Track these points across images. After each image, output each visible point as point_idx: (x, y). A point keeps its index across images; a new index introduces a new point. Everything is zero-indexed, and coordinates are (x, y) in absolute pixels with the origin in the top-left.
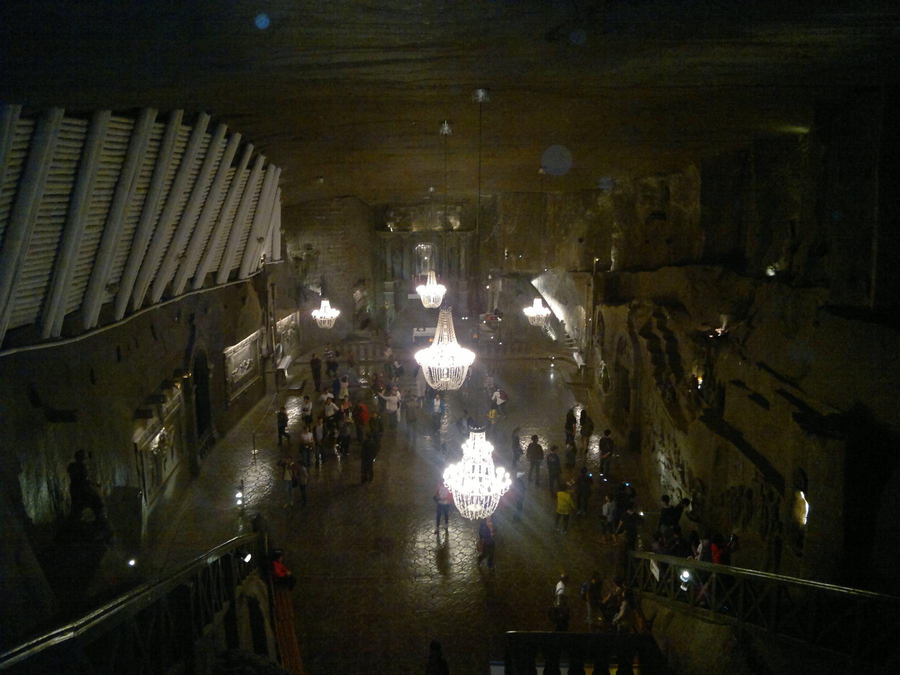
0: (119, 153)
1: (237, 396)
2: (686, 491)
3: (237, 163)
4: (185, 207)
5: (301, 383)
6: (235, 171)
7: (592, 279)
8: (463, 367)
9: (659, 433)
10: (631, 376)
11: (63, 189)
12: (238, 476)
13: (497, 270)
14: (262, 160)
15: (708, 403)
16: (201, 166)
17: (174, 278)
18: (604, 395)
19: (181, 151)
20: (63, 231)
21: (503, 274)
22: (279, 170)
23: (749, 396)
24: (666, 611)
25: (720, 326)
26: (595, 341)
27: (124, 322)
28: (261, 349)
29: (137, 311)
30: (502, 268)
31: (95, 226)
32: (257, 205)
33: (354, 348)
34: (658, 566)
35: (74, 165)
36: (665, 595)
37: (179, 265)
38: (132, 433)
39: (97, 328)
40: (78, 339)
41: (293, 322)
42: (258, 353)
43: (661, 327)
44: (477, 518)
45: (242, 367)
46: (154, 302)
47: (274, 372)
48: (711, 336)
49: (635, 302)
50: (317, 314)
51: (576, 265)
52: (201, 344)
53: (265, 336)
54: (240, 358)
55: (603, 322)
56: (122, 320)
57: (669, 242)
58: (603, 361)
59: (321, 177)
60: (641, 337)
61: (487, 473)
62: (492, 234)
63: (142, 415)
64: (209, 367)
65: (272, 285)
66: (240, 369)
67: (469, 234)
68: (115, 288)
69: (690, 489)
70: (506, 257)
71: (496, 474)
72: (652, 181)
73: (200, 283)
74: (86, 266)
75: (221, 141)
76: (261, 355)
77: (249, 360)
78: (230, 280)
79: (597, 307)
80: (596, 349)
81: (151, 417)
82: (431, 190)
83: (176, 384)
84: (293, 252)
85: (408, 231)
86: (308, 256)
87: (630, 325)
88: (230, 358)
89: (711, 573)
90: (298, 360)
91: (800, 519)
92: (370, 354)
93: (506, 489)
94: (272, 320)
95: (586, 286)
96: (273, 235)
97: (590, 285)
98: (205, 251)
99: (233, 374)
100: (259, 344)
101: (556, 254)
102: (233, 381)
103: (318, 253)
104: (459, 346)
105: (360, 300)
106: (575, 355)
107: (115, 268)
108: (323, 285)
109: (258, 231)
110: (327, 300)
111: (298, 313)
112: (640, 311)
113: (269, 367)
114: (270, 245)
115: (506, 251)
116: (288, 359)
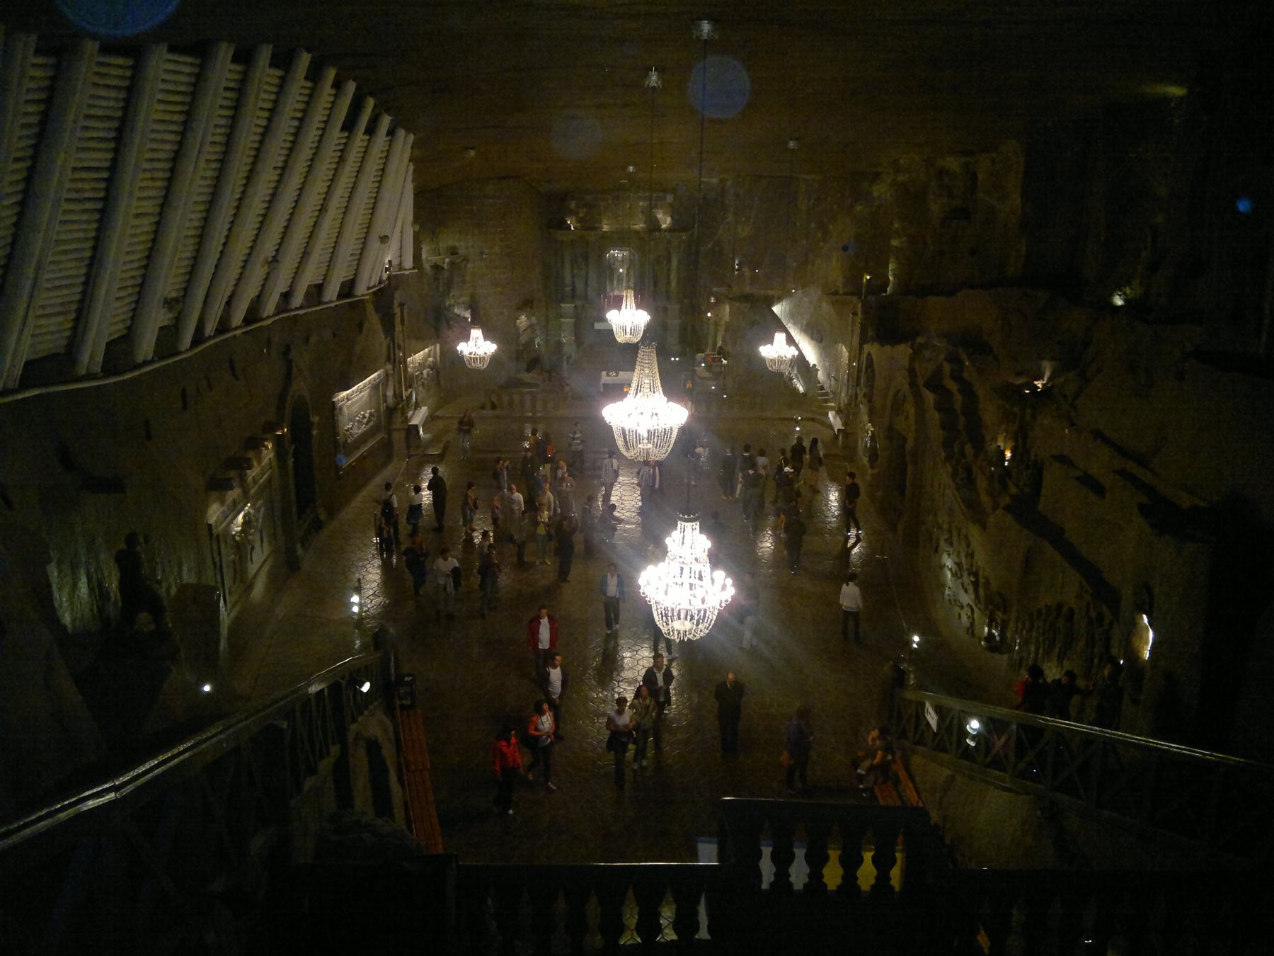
0: (178, 108)
1: (352, 463)
2: (980, 610)
3: (349, 126)
4: (276, 188)
5: (441, 445)
6: (348, 138)
7: (860, 305)
8: (671, 429)
9: (946, 526)
10: (910, 444)
11: (100, 160)
12: (354, 573)
13: (722, 290)
14: (386, 121)
15: (1017, 486)
16: (299, 129)
17: (261, 291)
18: (870, 471)
19: (269, 105)
20: (100, 221)
21: (731, 296)
22: (412, 137)
23: (1078, 479)
24: (947, 772)
25: (1040, 378)
26: (860, 397)
27: (189, 354)
28: (385, 396)
29: (210, 338)
30: (730, 286)
31: (146, 214)
32: (378, 188)
33: (516, 398)
34: (936, 712)
35: (115, 124)
36: (944, 750)
37: (268, 274)
38: (203, 512)
39: (151, 362)
40: (127, 376)
41: (430, 359)
42: (382, 402)
43: (957, 378)
44: (686, 639)
45: (358, 421)
46: (234, 326)
47: (405, 429)
48: (1027, 392)
49: (920, 340)
50: (464, 348)
51: (838, 284)
52: (301, 387)
53: (391, 379)
54: (355, 408)
55: (873, 371)
56: (187, 351)
57: (973, 252)
58: (870, 424)
59: (472, 149)
60: (927, 392)
61: (700, 578)
62: (717, 237)
63: (218, 485)
64: (311, 419)
65: (401, 305)
66: (356, 424)
67: (684, 236)
68: (177, 304)
69: (986, 607)
70: (737, 270)
71: (713, 580)
72: (953, 163)
73: (298, 300)
74: (134, 273)
75: (327, 90)
76: (385, 405)
77: (368, 411)
78: (340, 296)
79: (865, 346)
80: (861, 406)
81: (232, 488)
82: (631, 170)
83: (266, 443)
84: (429, 258)
85: (595, 229)
86: (452, 264)
87: (912, 372)
88: (341, 408)
89: (1008, 724)
90: (437, 413)
91: (1139, 652)
92: (539, 406)
93: (726, 601)
94: (401, 354)
95: (851, 315)
96: (402, 232)
97: (857, 315)
98: (305, 254)
99: (345, 430)
100: (383, 390)
101: (809, 267)
102: (347, 440)
103: (466, 259)
104: (666, 399)
105: (525, 330)
106: (831, 415)
107: (176, 276)
108: (473, 306)
109: (378, 230)
110: (479, 328)
111: (438, 346)
112: (927, 354)
113: (397, 423)
114: (399, 247)
115: (737, 262)
116: (424, 411)
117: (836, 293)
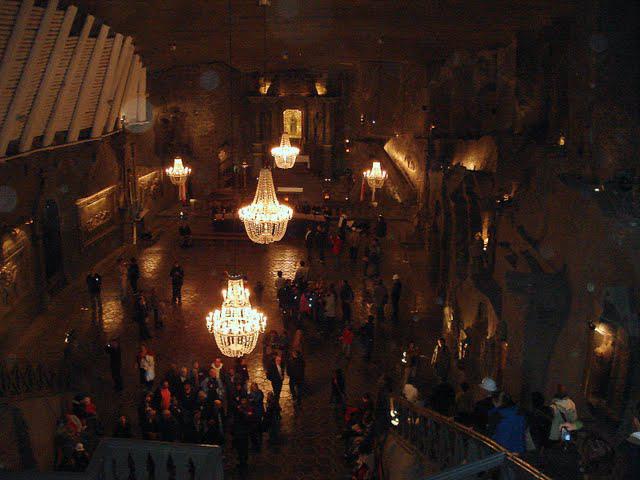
28: (118, 201)
57: (494, 111)
67: (334, 101)
73: (50, 139)
78: (80, 138)
87: (444, 189)
103: (185, 114)
117: (420, 137)
